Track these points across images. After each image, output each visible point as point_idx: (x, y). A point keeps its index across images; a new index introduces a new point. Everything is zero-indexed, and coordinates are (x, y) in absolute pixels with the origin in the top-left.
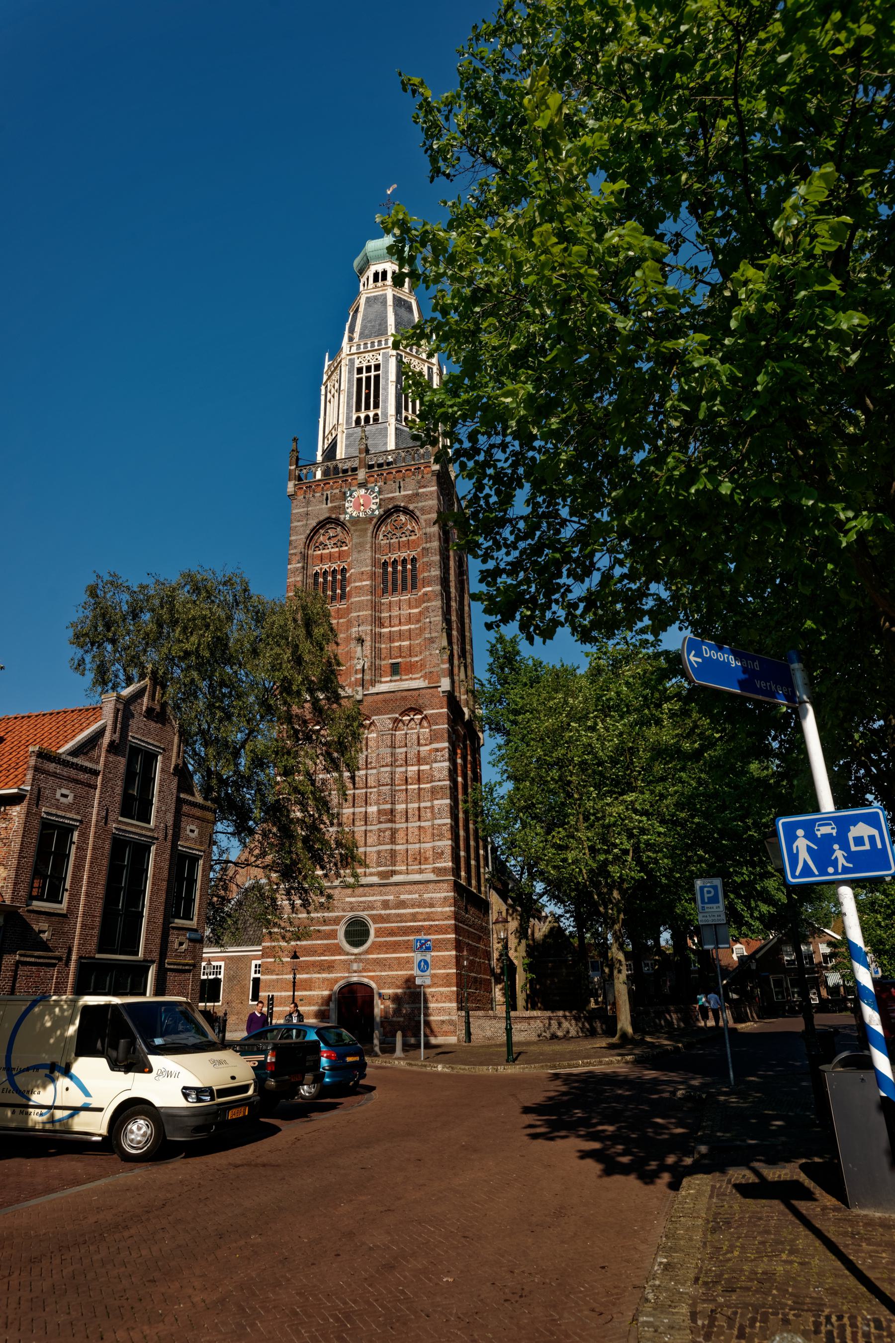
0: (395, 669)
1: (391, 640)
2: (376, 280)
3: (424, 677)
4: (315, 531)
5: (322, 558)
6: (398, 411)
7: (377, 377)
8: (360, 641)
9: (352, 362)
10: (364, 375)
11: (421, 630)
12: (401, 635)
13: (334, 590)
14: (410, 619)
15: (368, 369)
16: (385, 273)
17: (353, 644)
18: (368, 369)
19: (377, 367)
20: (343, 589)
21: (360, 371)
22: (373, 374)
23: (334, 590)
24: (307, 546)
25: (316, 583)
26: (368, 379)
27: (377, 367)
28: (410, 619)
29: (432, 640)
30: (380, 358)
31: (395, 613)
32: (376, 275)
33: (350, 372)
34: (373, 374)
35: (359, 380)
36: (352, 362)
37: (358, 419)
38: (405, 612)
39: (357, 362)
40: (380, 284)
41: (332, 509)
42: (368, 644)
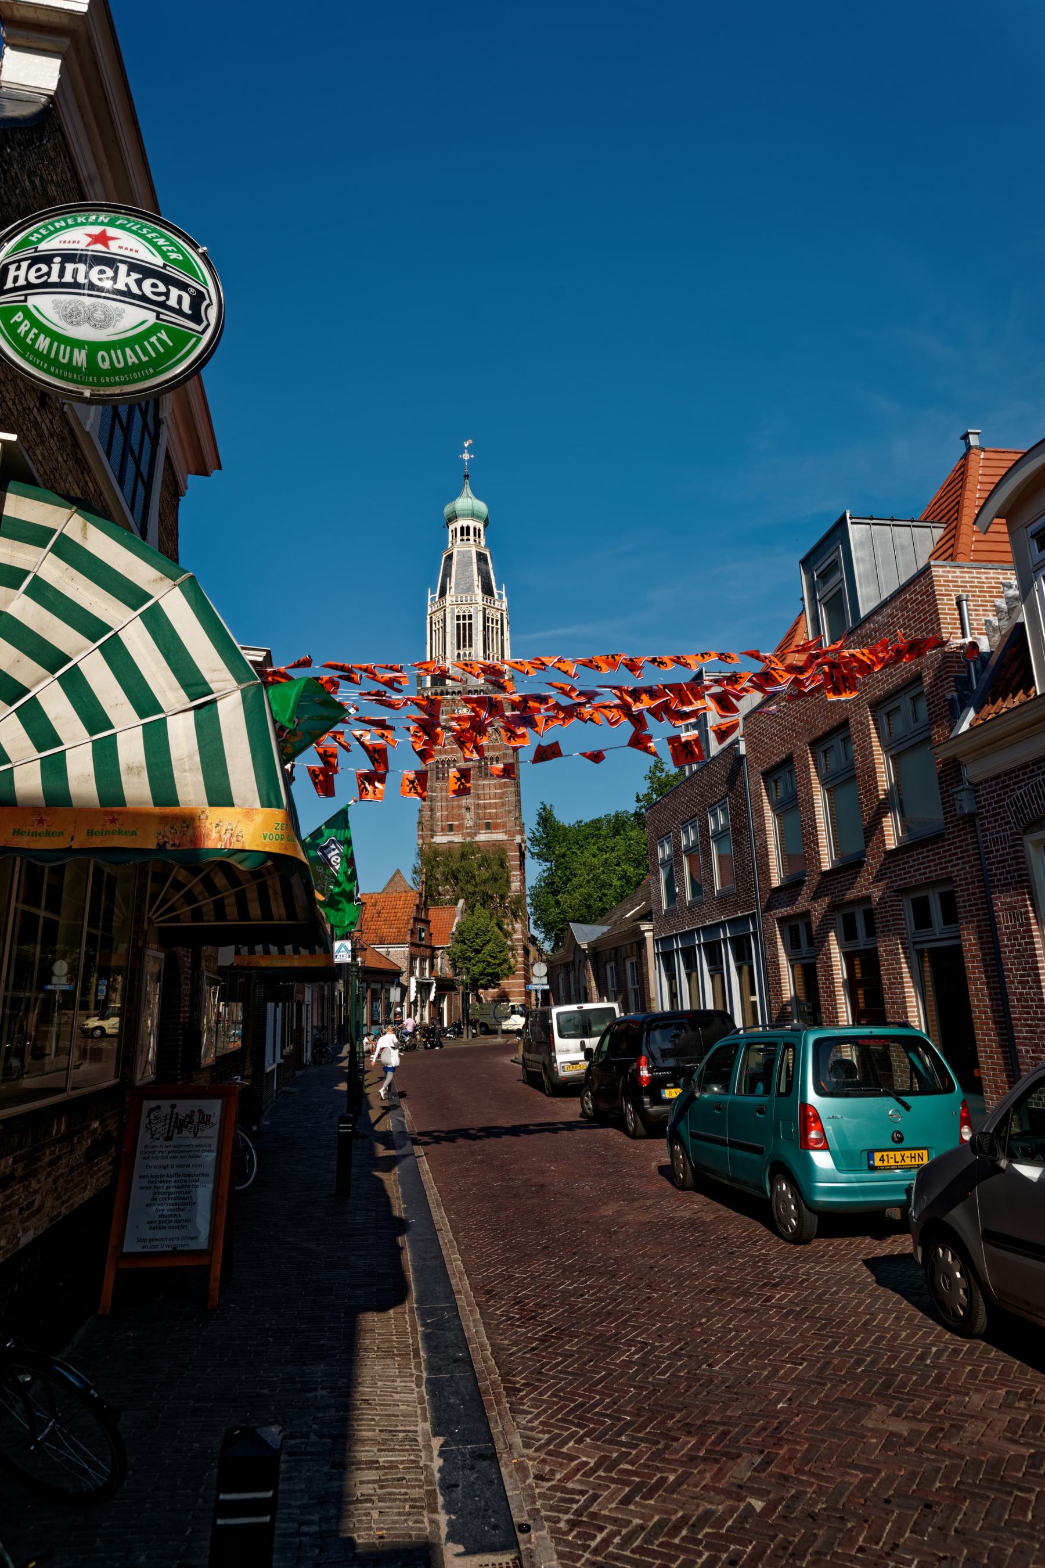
0: (488, 826)
1: (486, 809)
2: (462, 534)
3: (506, 833)
6: (485, 652)
7: (470, 624)
8: (468, 809)
9: (453, 610)
10: (461, 622)
11: (503, 804)
12: (491, 806)
14: (495, 796)
15: (464, 617)
16: (468, 528)
17: (464, 810)
21: (458, 618)
22: (467, 622)
25: (437, 767)
26: (464, 624)
27: (470, 617)
28: (495, 796)
29: (509, 812)
31: (487, 791)
32: (462, 528)
33: (452, 618)
34: (467, 622)
35: (458, 625)
36: (453, 610)
37: (459, 654)
38: (493, 791)
40: (465, 537)
42: (472, 810)
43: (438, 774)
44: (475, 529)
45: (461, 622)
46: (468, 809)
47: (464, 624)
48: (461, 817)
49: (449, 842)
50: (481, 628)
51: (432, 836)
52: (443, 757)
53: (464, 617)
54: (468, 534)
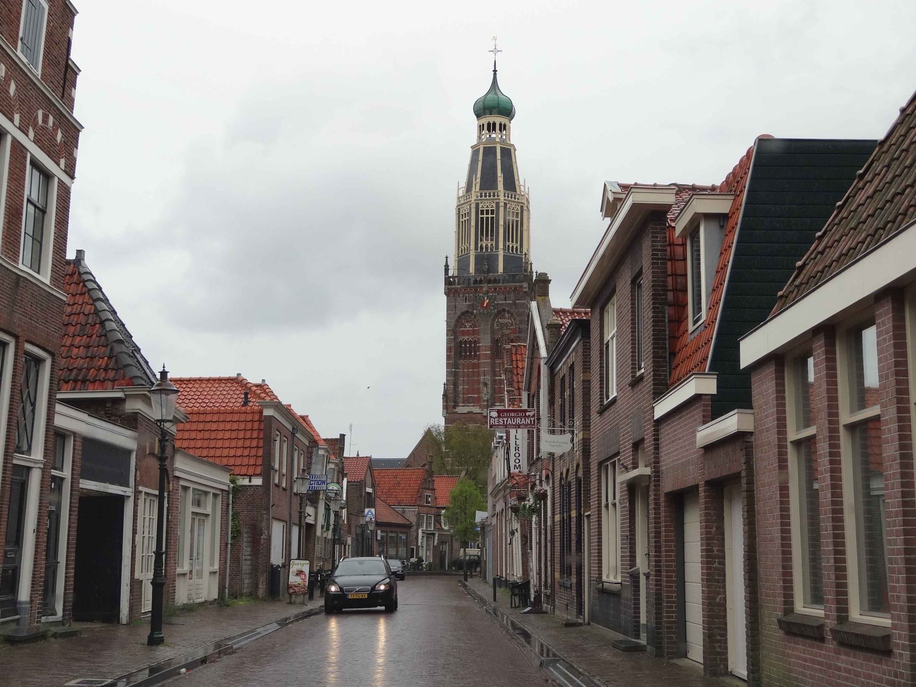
4: (460, 317)
5: (463, 333)
8: (486, 384)
9: (477, 205)
10: (485, 216)
13: (470, 353)
16: (494, 124)
18: (487, 214)
19: (492, 212)
20: (475, 353)
22: (490, 216)
23: (470, 353)
24: (456, 326)
26: (487, 218)
30: (494, 205)
32: (489, 124)
34: (490, 216)
39: (480, 206)
41: (469, 306)
43: (461, 352)
44: (500, 124)
45: (485, 216)
46: (486, 384)
47: (487, 218)
48: (478, 391)
49: (469, 413)
50: (501, 222)
51: (454, 407)
52: (466, 338)
53: (487, 211)
54: (494, 129)
